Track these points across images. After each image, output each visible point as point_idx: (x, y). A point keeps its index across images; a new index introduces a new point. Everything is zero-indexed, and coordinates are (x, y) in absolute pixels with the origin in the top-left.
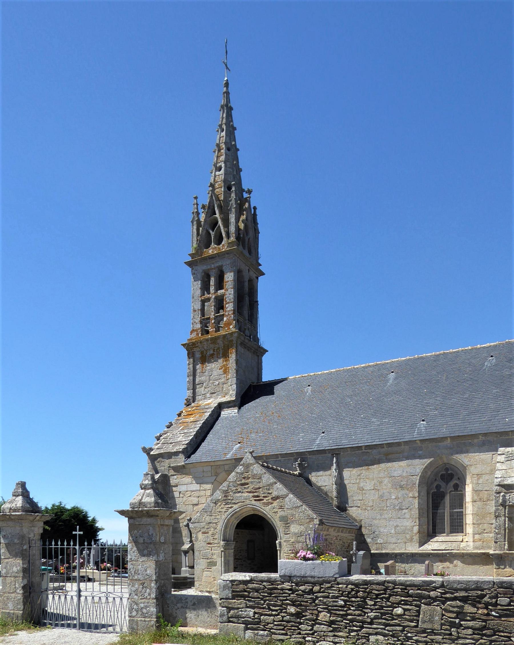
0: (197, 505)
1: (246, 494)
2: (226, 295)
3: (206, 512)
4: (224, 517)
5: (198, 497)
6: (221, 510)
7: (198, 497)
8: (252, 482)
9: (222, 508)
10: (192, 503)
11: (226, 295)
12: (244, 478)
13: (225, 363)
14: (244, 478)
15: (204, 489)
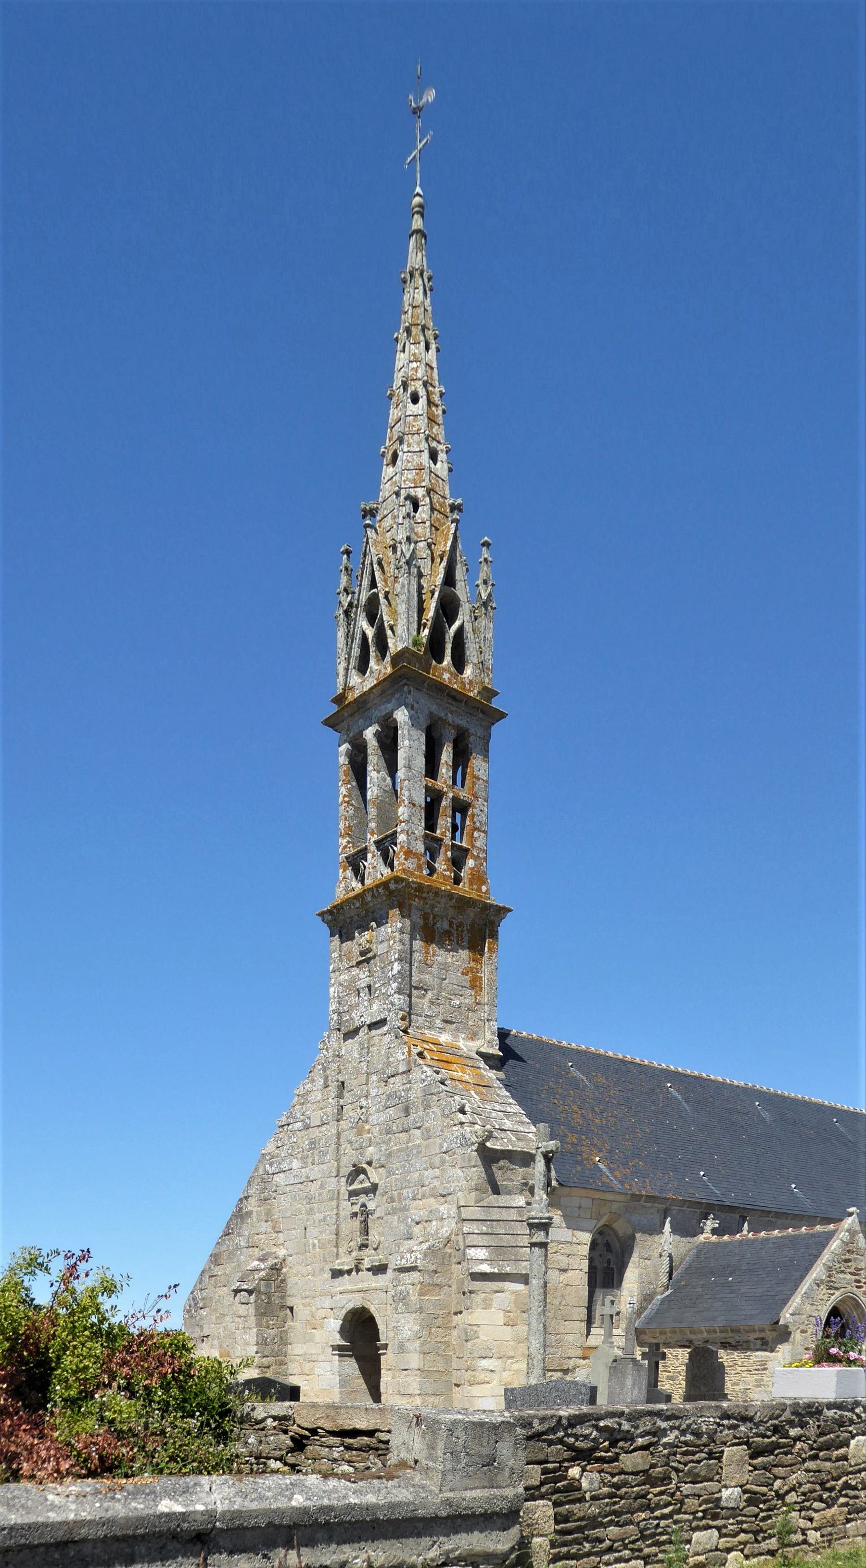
0: (565, 1271)
1: (849, 1276)
2: (474, 807)
3: (808, 1298)
4: (825, 1308)
5: (569, 1255)
6: (823, 1297)
7: (569, 1255)
8: (855, 1259)
9: (824, 1294)
10: (558, 1267)
11: (474, 807)
12: (849, 1251)
13: (472, 964)
14: (849, 1251)
15: (577, 1241)
